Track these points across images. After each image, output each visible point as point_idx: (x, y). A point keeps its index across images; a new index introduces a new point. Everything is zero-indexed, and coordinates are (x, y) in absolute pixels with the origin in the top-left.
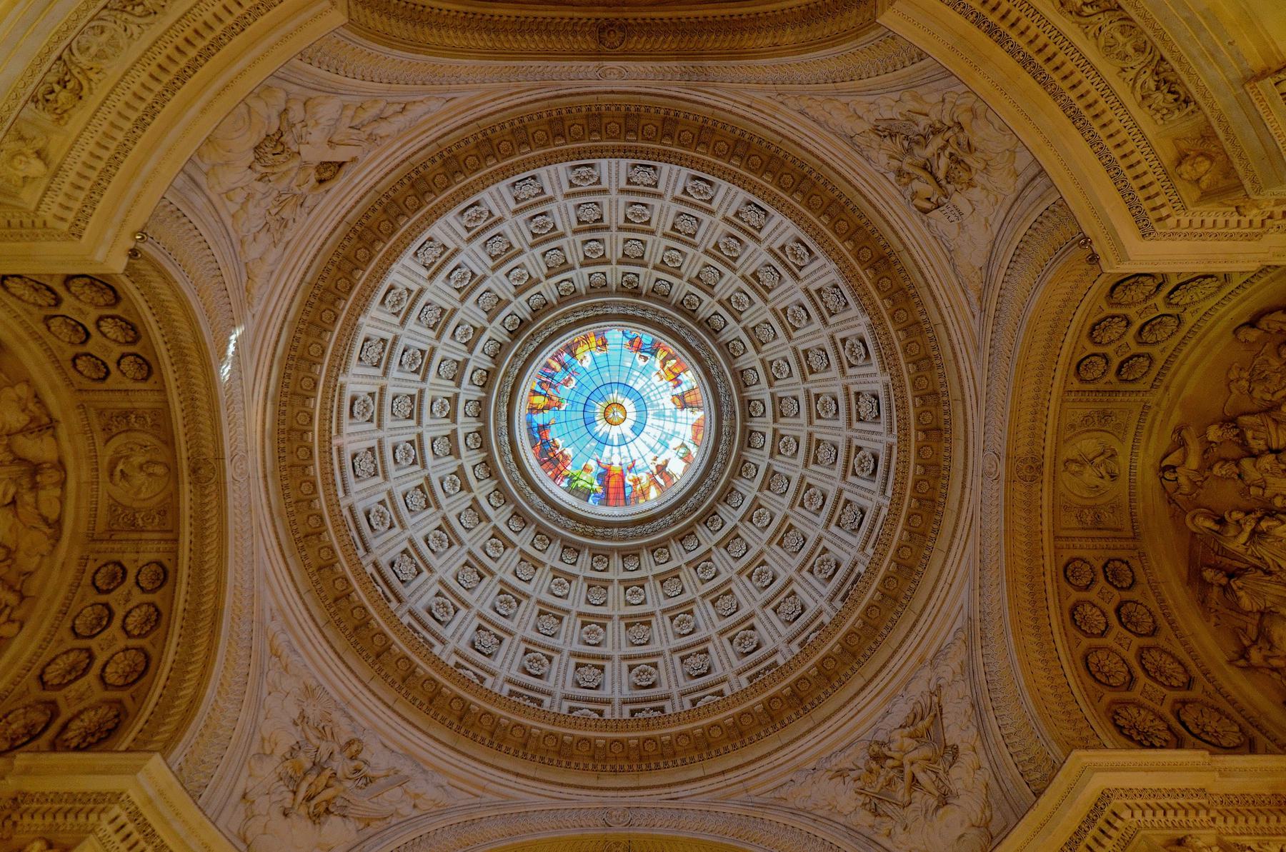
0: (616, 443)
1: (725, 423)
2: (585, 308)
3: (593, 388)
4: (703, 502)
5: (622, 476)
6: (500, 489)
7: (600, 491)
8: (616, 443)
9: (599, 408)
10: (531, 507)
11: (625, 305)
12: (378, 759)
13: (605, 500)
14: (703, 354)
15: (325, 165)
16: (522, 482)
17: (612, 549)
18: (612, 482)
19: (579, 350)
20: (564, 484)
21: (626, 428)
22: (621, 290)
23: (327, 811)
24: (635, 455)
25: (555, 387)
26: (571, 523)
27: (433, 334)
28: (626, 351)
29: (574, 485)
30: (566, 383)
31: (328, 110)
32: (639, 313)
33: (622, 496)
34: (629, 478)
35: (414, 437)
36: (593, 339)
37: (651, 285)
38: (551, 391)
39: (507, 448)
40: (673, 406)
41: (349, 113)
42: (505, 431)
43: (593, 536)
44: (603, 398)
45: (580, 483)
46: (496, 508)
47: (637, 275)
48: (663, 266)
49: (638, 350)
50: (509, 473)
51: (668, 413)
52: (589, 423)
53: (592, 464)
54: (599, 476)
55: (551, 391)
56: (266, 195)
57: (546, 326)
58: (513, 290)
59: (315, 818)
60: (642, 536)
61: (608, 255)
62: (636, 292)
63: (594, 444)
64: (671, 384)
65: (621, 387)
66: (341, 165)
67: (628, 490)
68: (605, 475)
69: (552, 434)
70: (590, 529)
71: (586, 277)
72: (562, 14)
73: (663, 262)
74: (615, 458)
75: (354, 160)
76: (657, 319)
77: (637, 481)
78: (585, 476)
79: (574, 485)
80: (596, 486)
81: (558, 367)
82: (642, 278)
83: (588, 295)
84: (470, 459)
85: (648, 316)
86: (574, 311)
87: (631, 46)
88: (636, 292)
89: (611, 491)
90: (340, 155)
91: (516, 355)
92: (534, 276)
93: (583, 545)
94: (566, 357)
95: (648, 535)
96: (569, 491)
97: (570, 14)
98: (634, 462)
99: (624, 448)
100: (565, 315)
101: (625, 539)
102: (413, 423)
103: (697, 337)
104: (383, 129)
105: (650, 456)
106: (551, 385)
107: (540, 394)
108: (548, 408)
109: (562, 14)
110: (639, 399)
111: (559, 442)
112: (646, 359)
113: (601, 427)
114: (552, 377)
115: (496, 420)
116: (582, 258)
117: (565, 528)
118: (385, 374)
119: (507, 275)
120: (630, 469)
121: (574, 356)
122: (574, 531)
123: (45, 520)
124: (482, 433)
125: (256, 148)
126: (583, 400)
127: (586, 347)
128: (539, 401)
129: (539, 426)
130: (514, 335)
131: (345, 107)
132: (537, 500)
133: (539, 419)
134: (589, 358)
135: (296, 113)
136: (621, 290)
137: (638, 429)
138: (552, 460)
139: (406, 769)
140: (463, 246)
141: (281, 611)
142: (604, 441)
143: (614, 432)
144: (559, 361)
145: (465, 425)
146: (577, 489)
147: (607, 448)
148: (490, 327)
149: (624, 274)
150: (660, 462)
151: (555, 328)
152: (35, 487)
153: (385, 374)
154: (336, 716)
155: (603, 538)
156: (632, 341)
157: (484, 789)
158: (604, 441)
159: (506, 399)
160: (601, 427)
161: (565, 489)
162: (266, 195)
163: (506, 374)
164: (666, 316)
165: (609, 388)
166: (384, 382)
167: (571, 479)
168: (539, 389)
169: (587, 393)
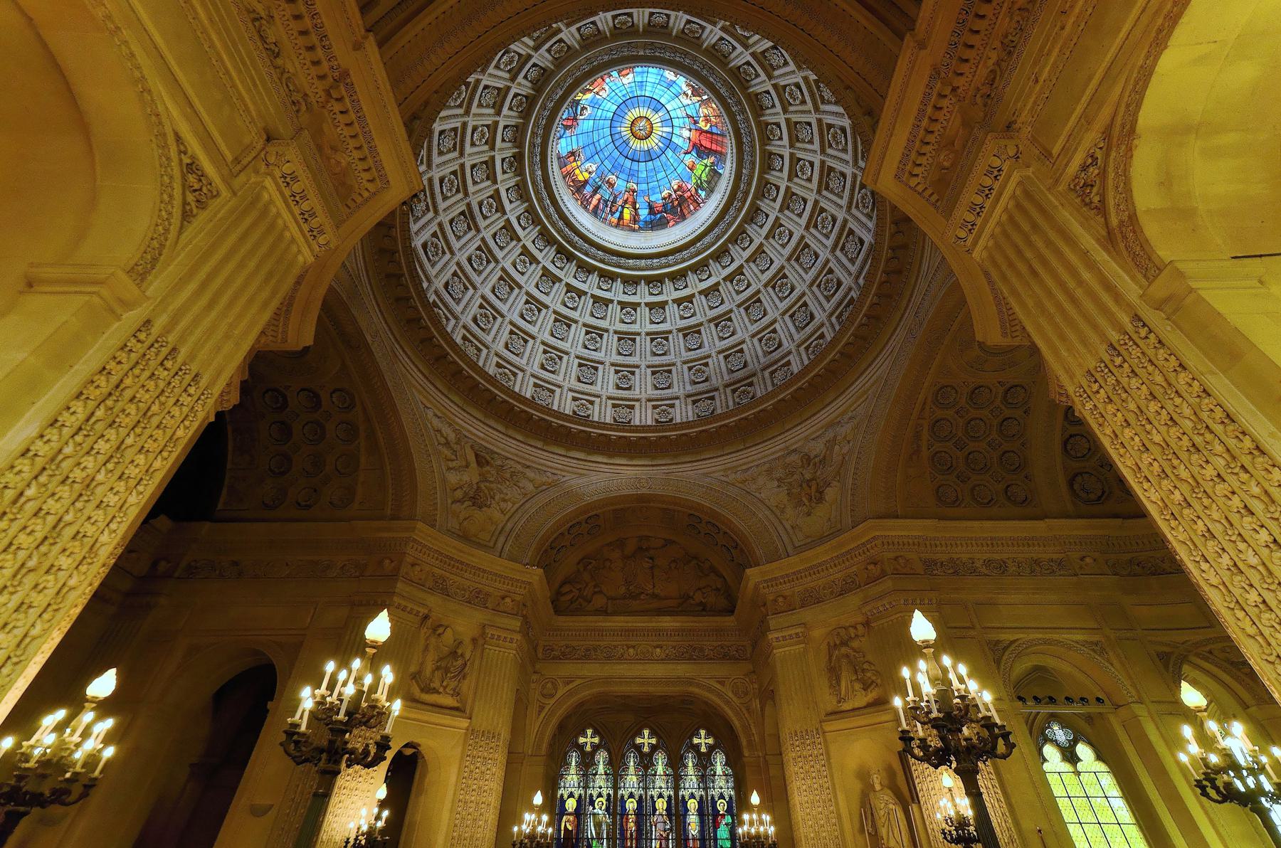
0: (669, 129)
1: (641, 53)
2: (540, 200)
3: (616, 153)
4: (725, 81)
5: (701, 131)
6: (695, 269)
7: (712, 159)
8: (669, 129)
9: (636, 144)
10: (713, 244)
11: (532, 164)
12: (818, 448)
13: (720, 155)
14: (570, 81)
15: (479, 463)
16: (692, 250)
17: (740, 225)
18: (706, 143)
19: (581, 178)
20: (703, 194)
21: (655, 118)
22: (520, 172)
23: (821, 493)
24: (680, 113)
25: (616, 197)
26: (732, 211)
27: (574, 326)
28: (578, 130)
29: (705, 185)
30: (611, 185)
31: (453, 478)
32: (538, 150)
33: (720, 138)
34: (702, 124)
35: (648, 338)
36: (569, 167)
38: (620, 202)
39: (663, 260)
40: (631, 76)
41: (451, 464)
42: (649, 262)
43: (746, 193)
44: (626, 143)
45: (704, 177)
46: (710, 276)
47: (503, 160)
49: (575, 119)
50: (684, 261)
51: (638, 79)
52: (649, 156)
53: (688, 159)
54: (699, 156)
55: (620, 202)
56: (501, 492)
57: (559, 231)
58: (534, 266)
59: (820, 499)
60: (753, 147)
62: (518, 157)
63: (669, 153)
64: (607, 80)
65: (615, 124)
66: (477, 455)
67: (714, 130)
68: (700, 150)
69: (657, 198)
70: (739, 195)
71: (514, 205)
74: (683, 136)
75: (472, 447)
76: (540, 132)
77: (707, 120)
78: (699, 169)
79: (705, 185)
80: (708, 161)
81: (598, 196)
83: (529, 200)
84: (670, 293)
85: (539, 140)
86: (544, 209)
88: (518, 157)
89: (714, 147)
90: (472, 458)
91: (587, 254)
93: (753, 203)
94: (588, 190)
95: (753, 140)
96: (711, 191)
98: (688, 116)
99: (676, 122)
100: (548, 217)
101: (753, 163)
102: (638, 338)
103: (553, 91)
104: (452, 436)
105: (686, 101)
106: (614, 202)
107: (622, 213)
108: (634, 203)
110: (625, 104)
111: (665, 194)
112: (584, 108)
113: (653, 143)
114: (606, 201)
115: (640, 269)
117: (735, 218)
118: (602, 363)
120: (696, 122)
121: (586, 182)
122: (740, 210)
123: (665, 546)
124: (649, 280)
125: (480, 507)
126: (628, 163)
127: (577, 172)
128: (627, 214)
129: (650, 213)
130: (570, 257)
131: (449, 469)
132: (707, 239)
133: (644, 213)
134: (587, 165)
135: (459, 494)
137: (657, 106)
138: (678, 207)
139: (830, 435)
140: (507, 320)
141: (725, 470)
142: (668, 142)
143: (659, 130)
144: (592, 197)
145: (643, 295)
146: (708, 182)
147: (675, 139)
148: (566, 280)
150: (689, 92)
151: (561, 223)
152: (647, 549)
153: (602, 363)
154: (788, 460)
155: (749, 184)
156: (567, 127)
157: (865, 392)
158: (668, 142)
159: (623, 261)
160: (653, 143)
161: (708, 196)
162: (501, 492)
163: (602, 261)
164: (536, 124)
165: (617, 136)
166: (607, 364)
167: (699, 186)
168: (617, 215)
169: (622, 160)
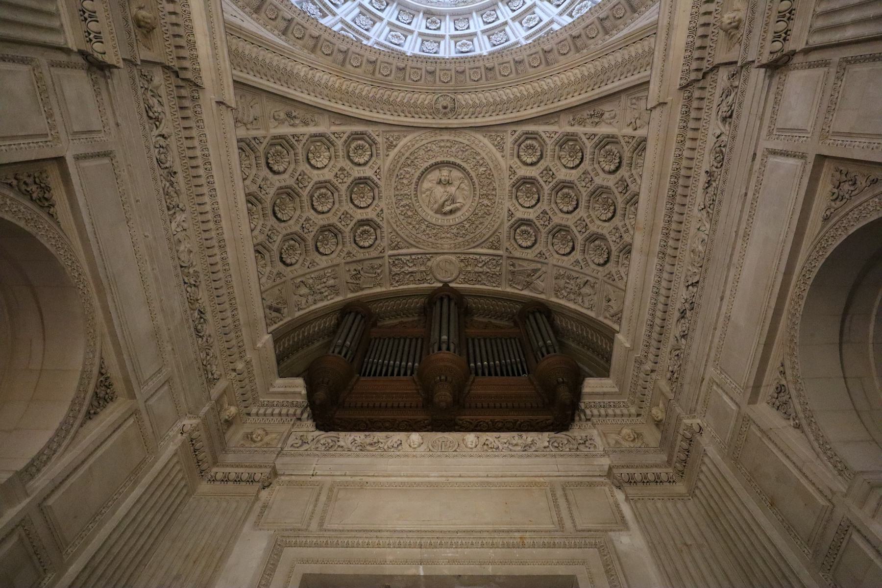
22: (441, 15)
37: (415, 20)
47: (427, 28)
48: (406, 33)
61: (452, 42)
72: (484, 120)
73: (406, 37)
82: (424, 26)
87: (430, 97)
88: (428, 14)
92: (517, 24)
97: (478, 120)
109: (484, 120)
116: (475, 40)
119: (541, 20)
136: (441, 15)
149: (439, 28)
